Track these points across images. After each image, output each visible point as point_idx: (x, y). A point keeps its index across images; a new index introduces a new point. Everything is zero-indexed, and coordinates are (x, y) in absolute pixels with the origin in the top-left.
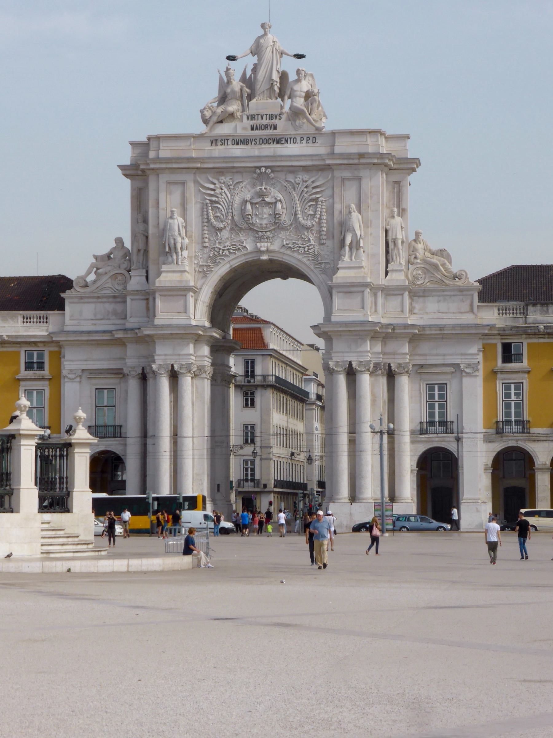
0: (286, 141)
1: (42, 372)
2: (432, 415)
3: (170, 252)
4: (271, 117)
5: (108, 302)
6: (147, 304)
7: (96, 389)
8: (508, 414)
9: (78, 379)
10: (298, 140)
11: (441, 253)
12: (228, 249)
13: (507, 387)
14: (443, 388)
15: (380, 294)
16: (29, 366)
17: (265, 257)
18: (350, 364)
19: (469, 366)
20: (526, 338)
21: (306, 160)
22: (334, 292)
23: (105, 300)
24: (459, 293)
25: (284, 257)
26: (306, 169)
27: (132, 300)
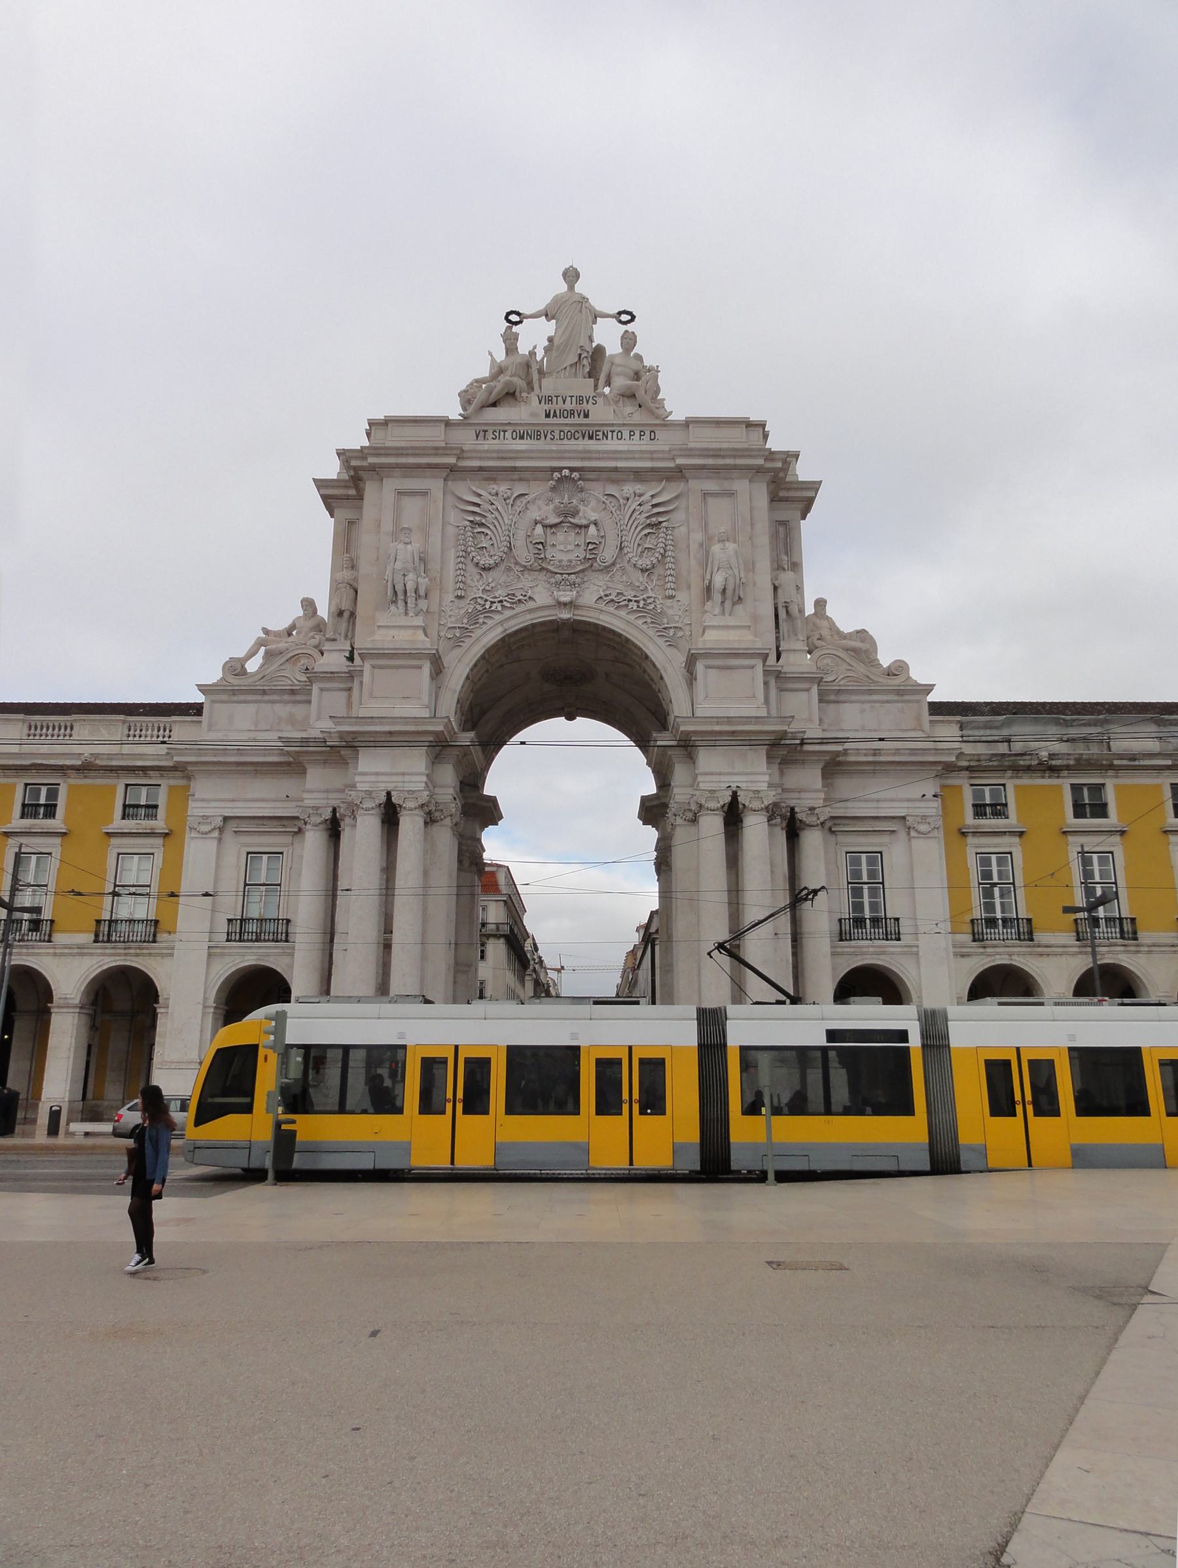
0: (605, 436)
1: (152, 823)
2: (858, 907)
3: (394, 602)
4: (580, 400)
5: (281, 702)
6: (350, 697)
7: (248, 853)
8: (989, 907)
9: (216, 834)
10: (626, 434)
11: (862, 634)
12: (501, 601)
13: (985, 862)
14: (876, 857)
15: (772, 683)
16: (129, 811)
17: (565, 615)
18: (735, 795)
19: (924, 817)
20: (1012, 778)
21: (642, 459)
22: (700, 667)
23: (275, 697)
24: (896, 698)
25: (601, 617)
26: (639, 475)
27: (322, 690)
